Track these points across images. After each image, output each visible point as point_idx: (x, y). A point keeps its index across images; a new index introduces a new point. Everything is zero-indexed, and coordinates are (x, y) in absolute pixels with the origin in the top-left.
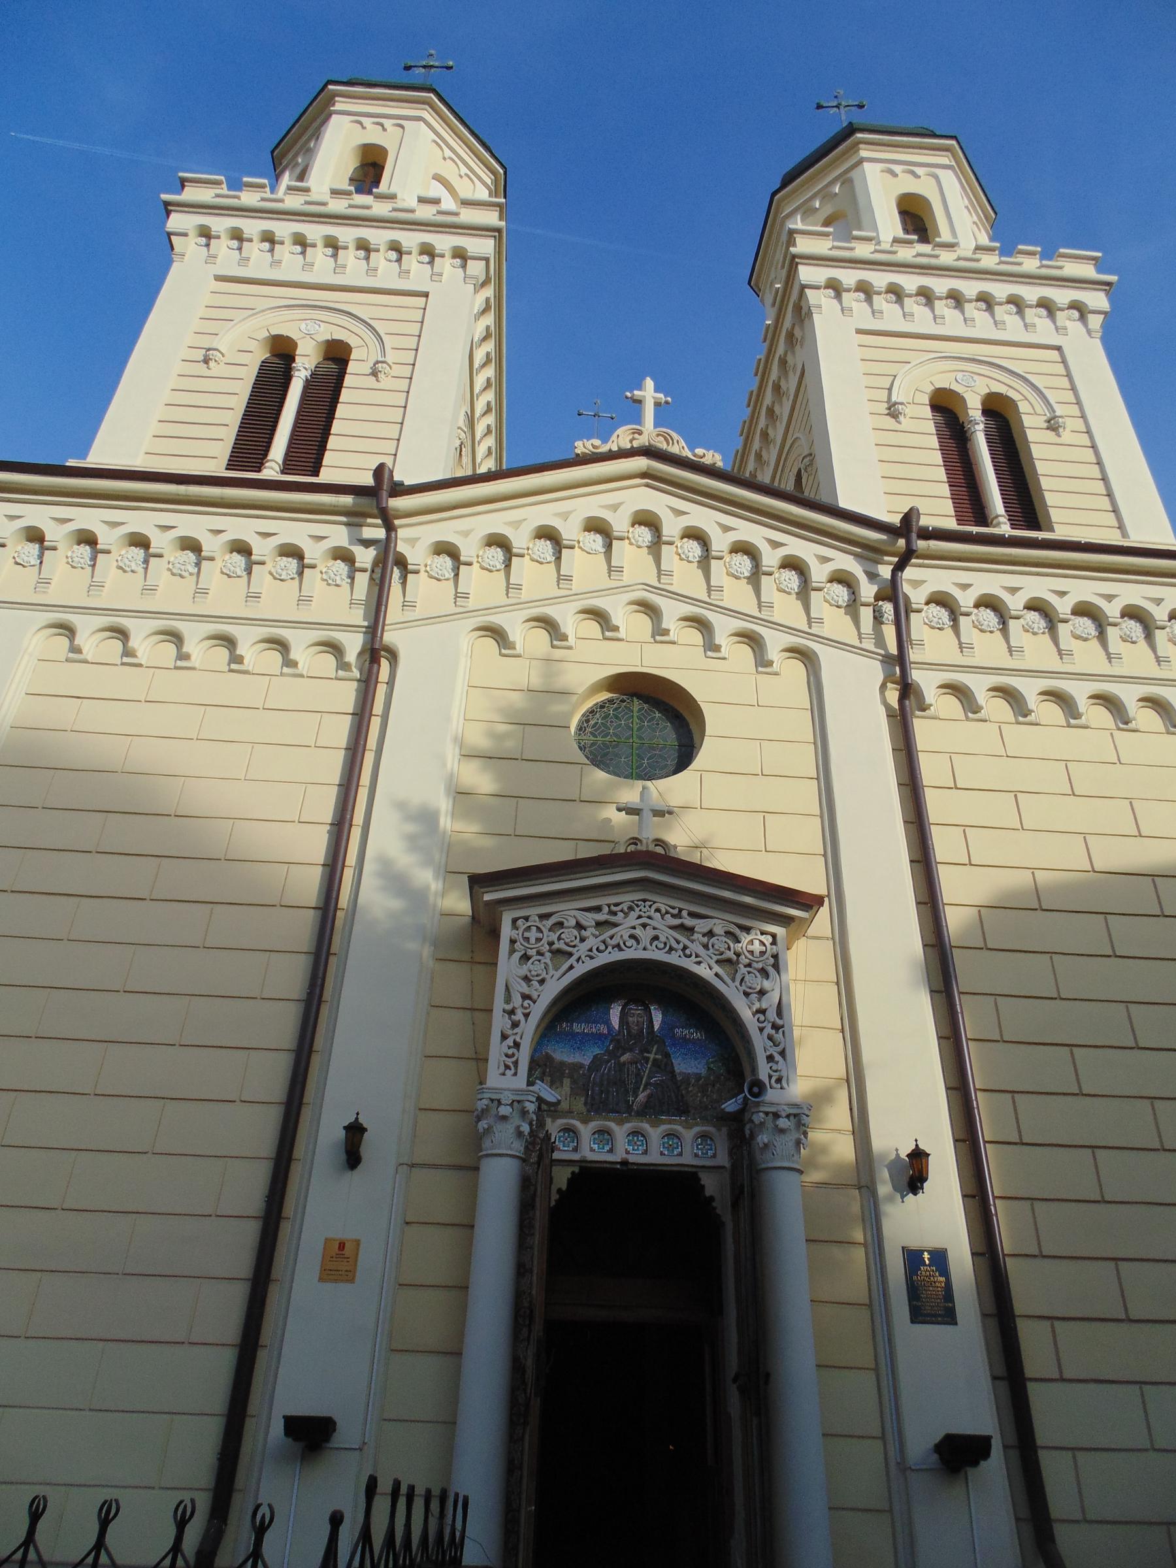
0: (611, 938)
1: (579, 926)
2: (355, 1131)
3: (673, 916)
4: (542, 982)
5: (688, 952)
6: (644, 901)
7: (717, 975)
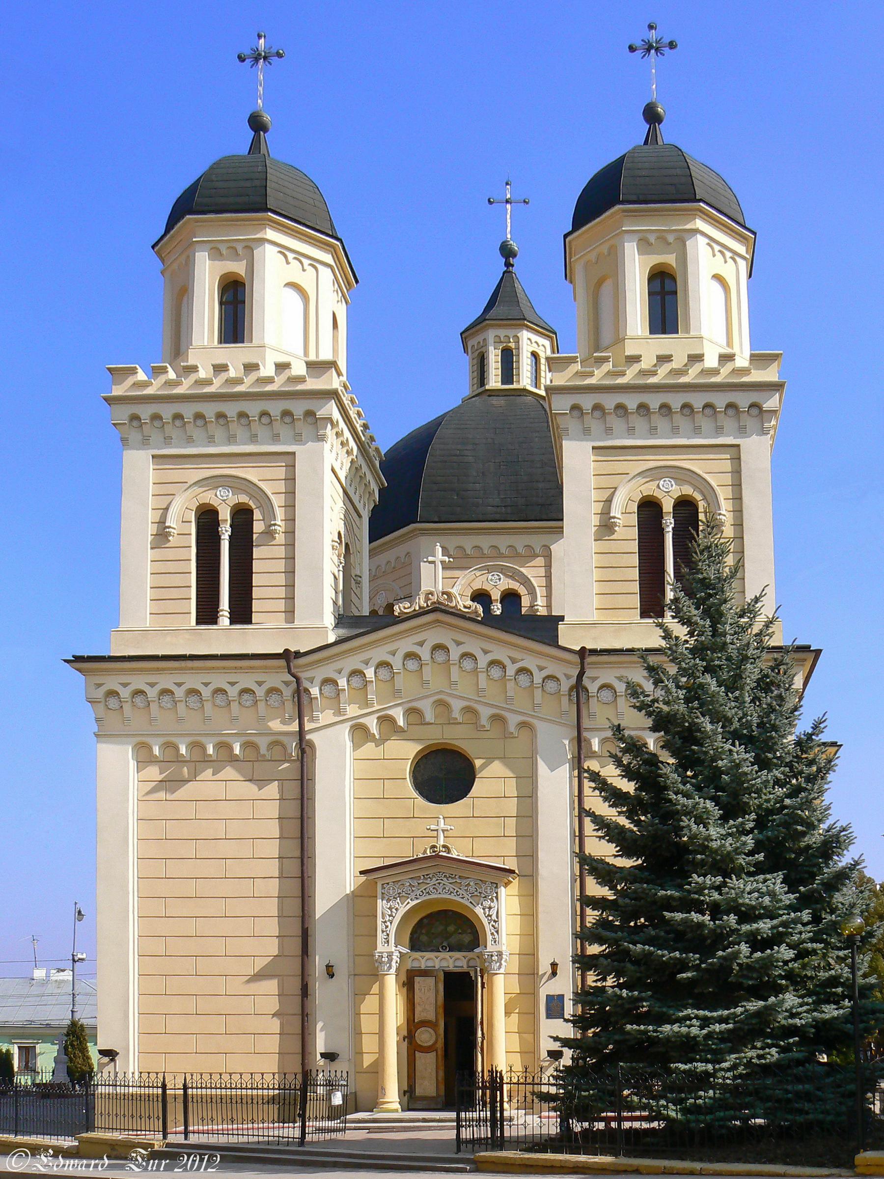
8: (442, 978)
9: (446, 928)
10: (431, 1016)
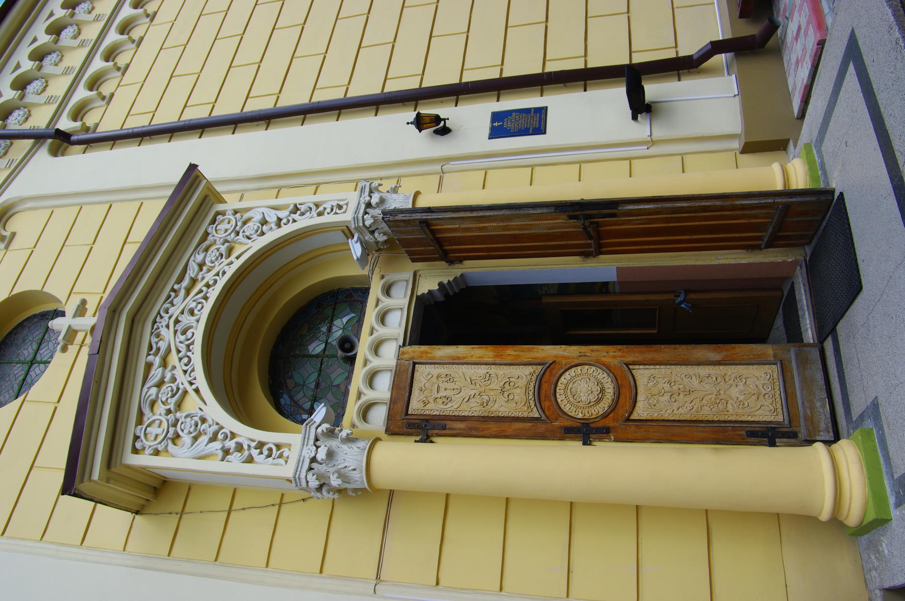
0: (179, 351)
1: (159, 385)
4: (204, 420)
5: (211, 283)
6: (155, 322)
7: (238, 258)
8: (424, 348)
10: (524, 375)
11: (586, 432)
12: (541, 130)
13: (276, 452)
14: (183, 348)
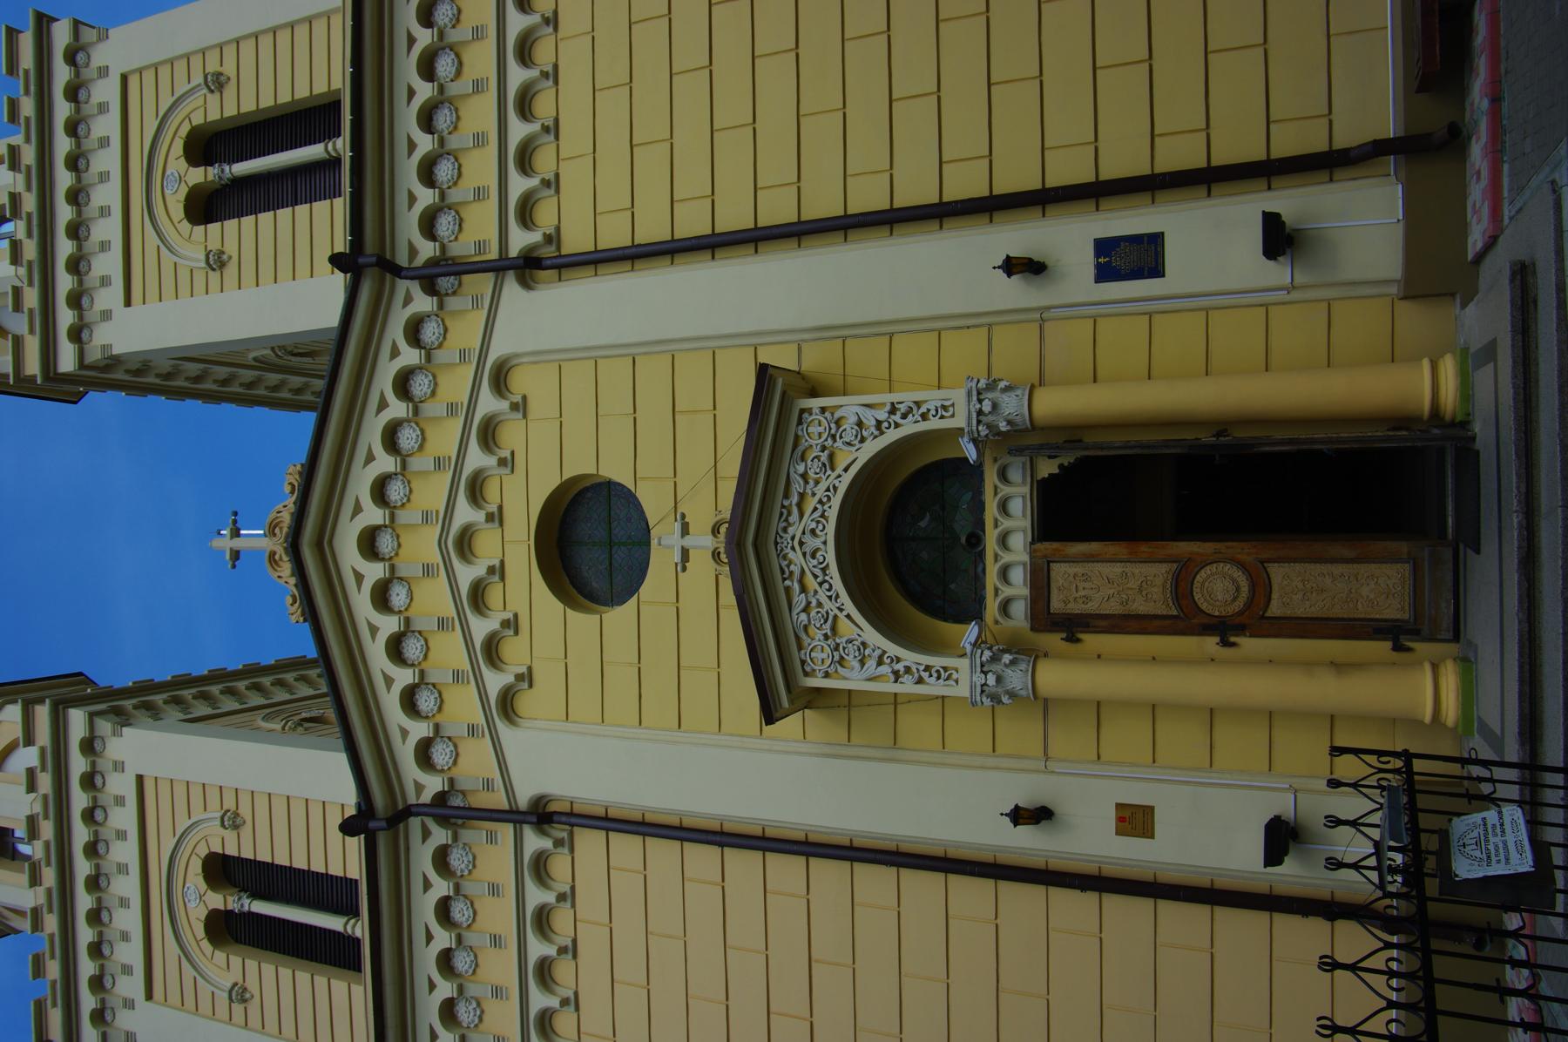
0: (816, 577)
1: (806, 610)
2: (1019, 816)
3: (789, 514)
4: (864, 644)
6: (776, 543)
7: (846, 470)
8: (1055, 545)
9: (910, 539)
10: (1159, 573)
11: (1225, 629)
12: (1157, 271)
13: (944, 674)
14: (817, 571)
